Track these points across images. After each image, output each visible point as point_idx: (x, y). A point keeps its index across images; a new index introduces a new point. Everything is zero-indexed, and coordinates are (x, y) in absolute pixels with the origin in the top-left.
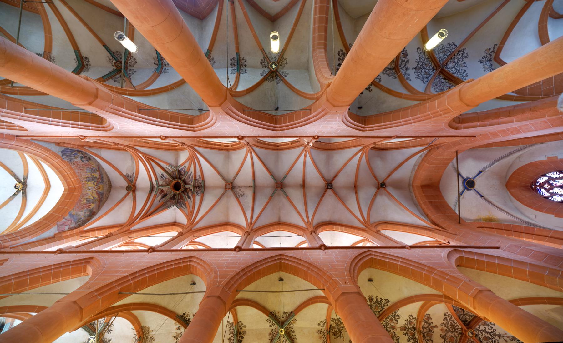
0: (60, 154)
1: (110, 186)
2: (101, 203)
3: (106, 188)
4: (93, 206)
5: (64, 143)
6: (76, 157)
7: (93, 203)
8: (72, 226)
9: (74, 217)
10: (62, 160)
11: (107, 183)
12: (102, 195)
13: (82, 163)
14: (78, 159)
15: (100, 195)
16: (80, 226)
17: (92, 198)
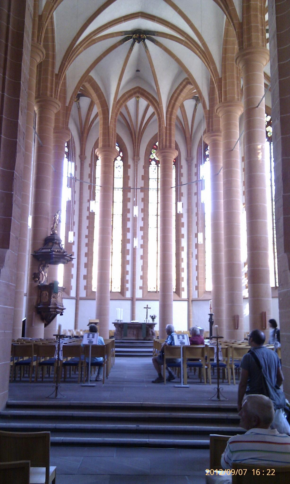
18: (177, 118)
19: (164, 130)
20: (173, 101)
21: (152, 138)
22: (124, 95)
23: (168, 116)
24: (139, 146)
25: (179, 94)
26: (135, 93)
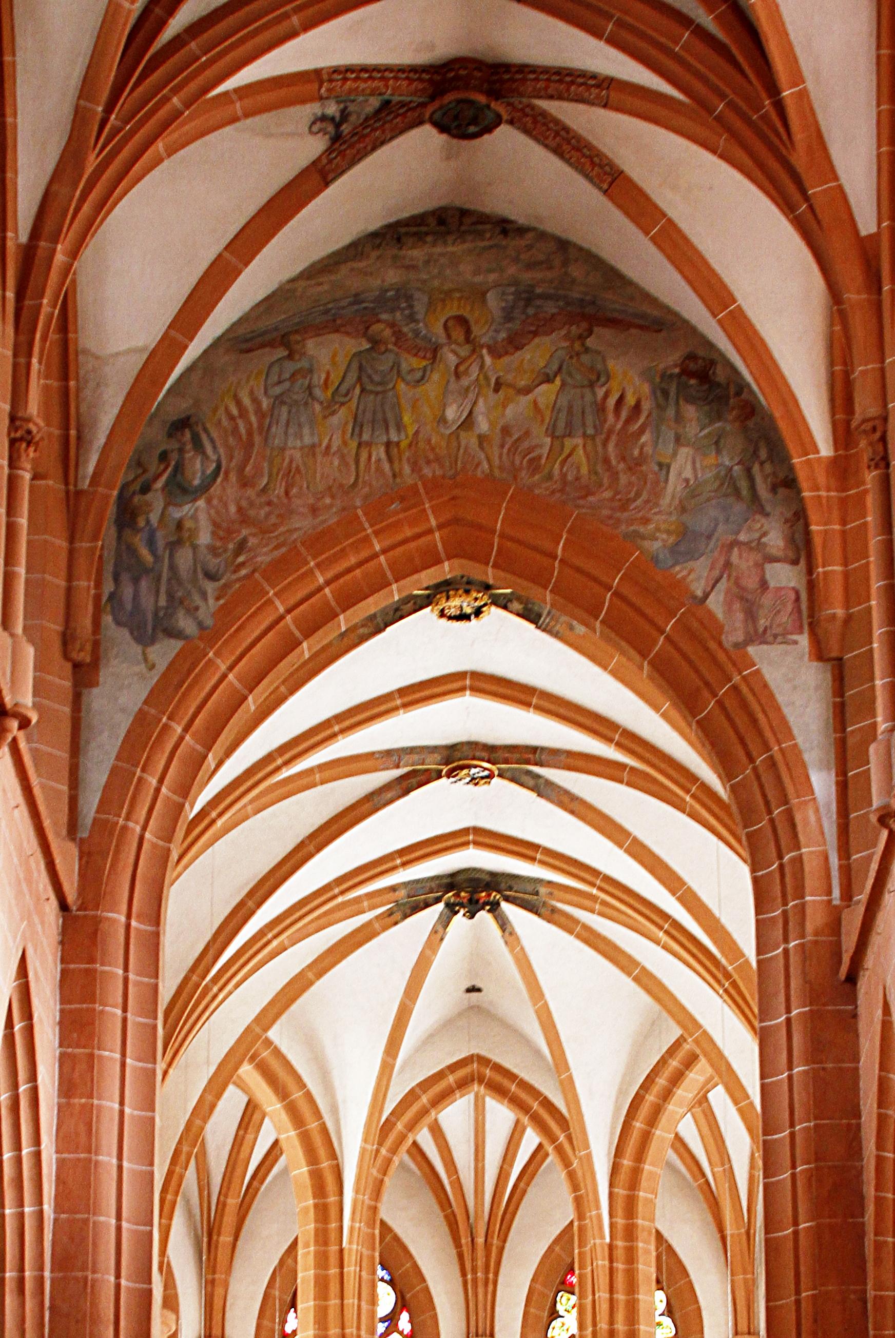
0: (164, 652)
1: (445, 223)
2: (612, 302)
3: (458, 263)
4: (629, 375)
5: (67, 639)
6: (180, 534)
7: (597, 376)
8: (775, 540)
9: (702, 523)
10: (210, 635)
11: (416, 254)
12: (528, 297)
13: (228, 491)
14: (198, 514)
15: (528, 316)
16: (788, 483)
17: (546, 393)
18: (680, 1144)
19: (602, 1263)
20: (638, 1125)
21: (557, 1241)
22: (411, 1097)
23: (620, 1191)
24: (491, 1283)
25: (667, 1095)
26: (463, 1085)
